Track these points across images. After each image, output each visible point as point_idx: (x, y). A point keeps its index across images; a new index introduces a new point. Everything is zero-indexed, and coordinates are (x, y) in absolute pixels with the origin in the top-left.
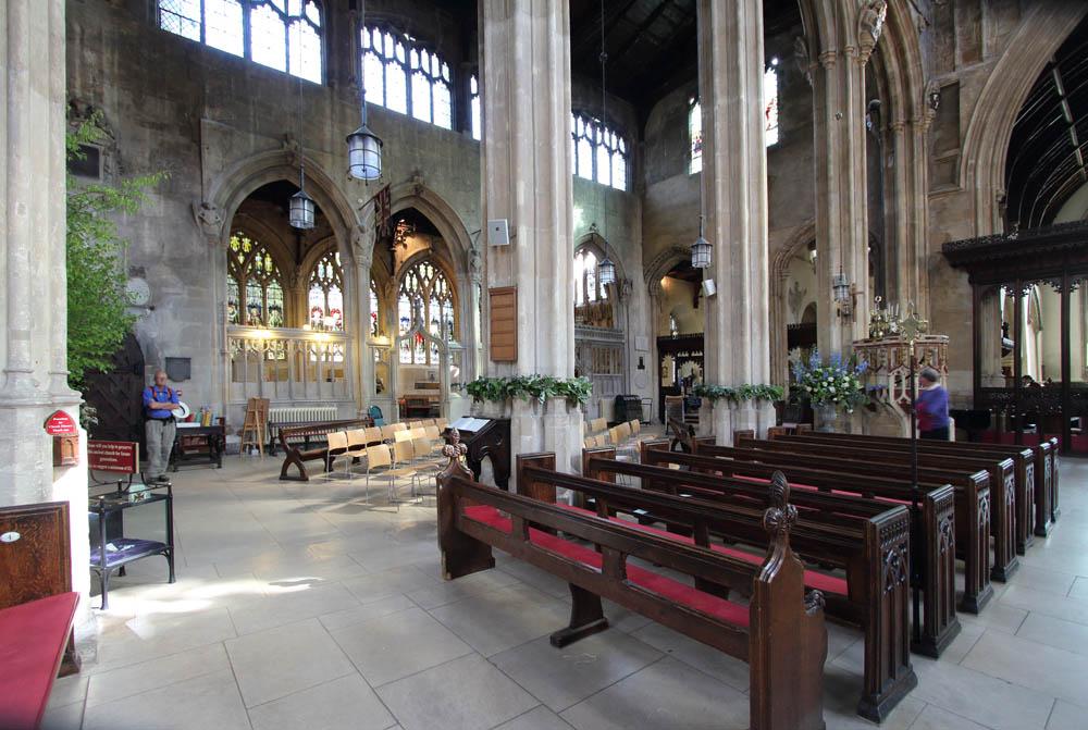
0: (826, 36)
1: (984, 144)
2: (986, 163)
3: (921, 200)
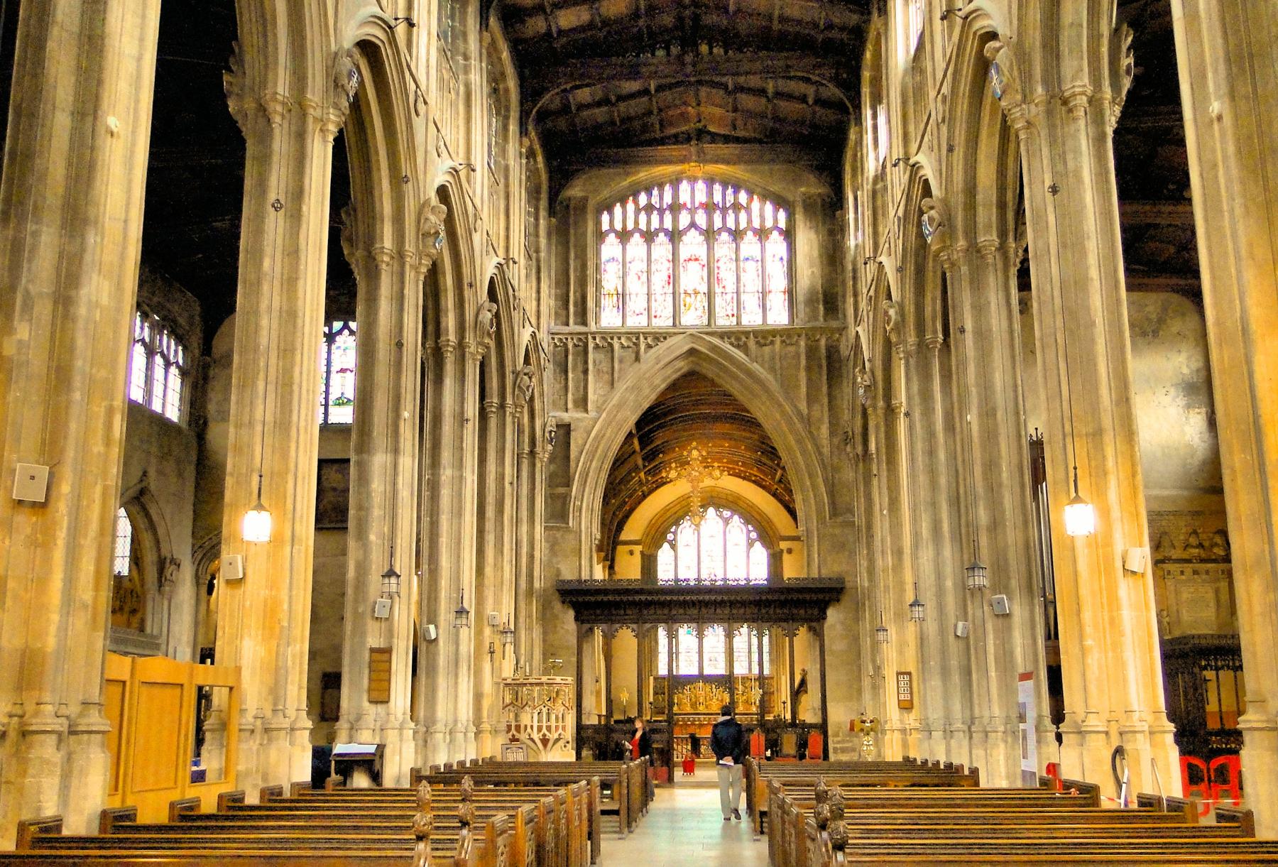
0: (491, 388)
1: (587, 490)
2: (588, 505)
3: (538, 529)
